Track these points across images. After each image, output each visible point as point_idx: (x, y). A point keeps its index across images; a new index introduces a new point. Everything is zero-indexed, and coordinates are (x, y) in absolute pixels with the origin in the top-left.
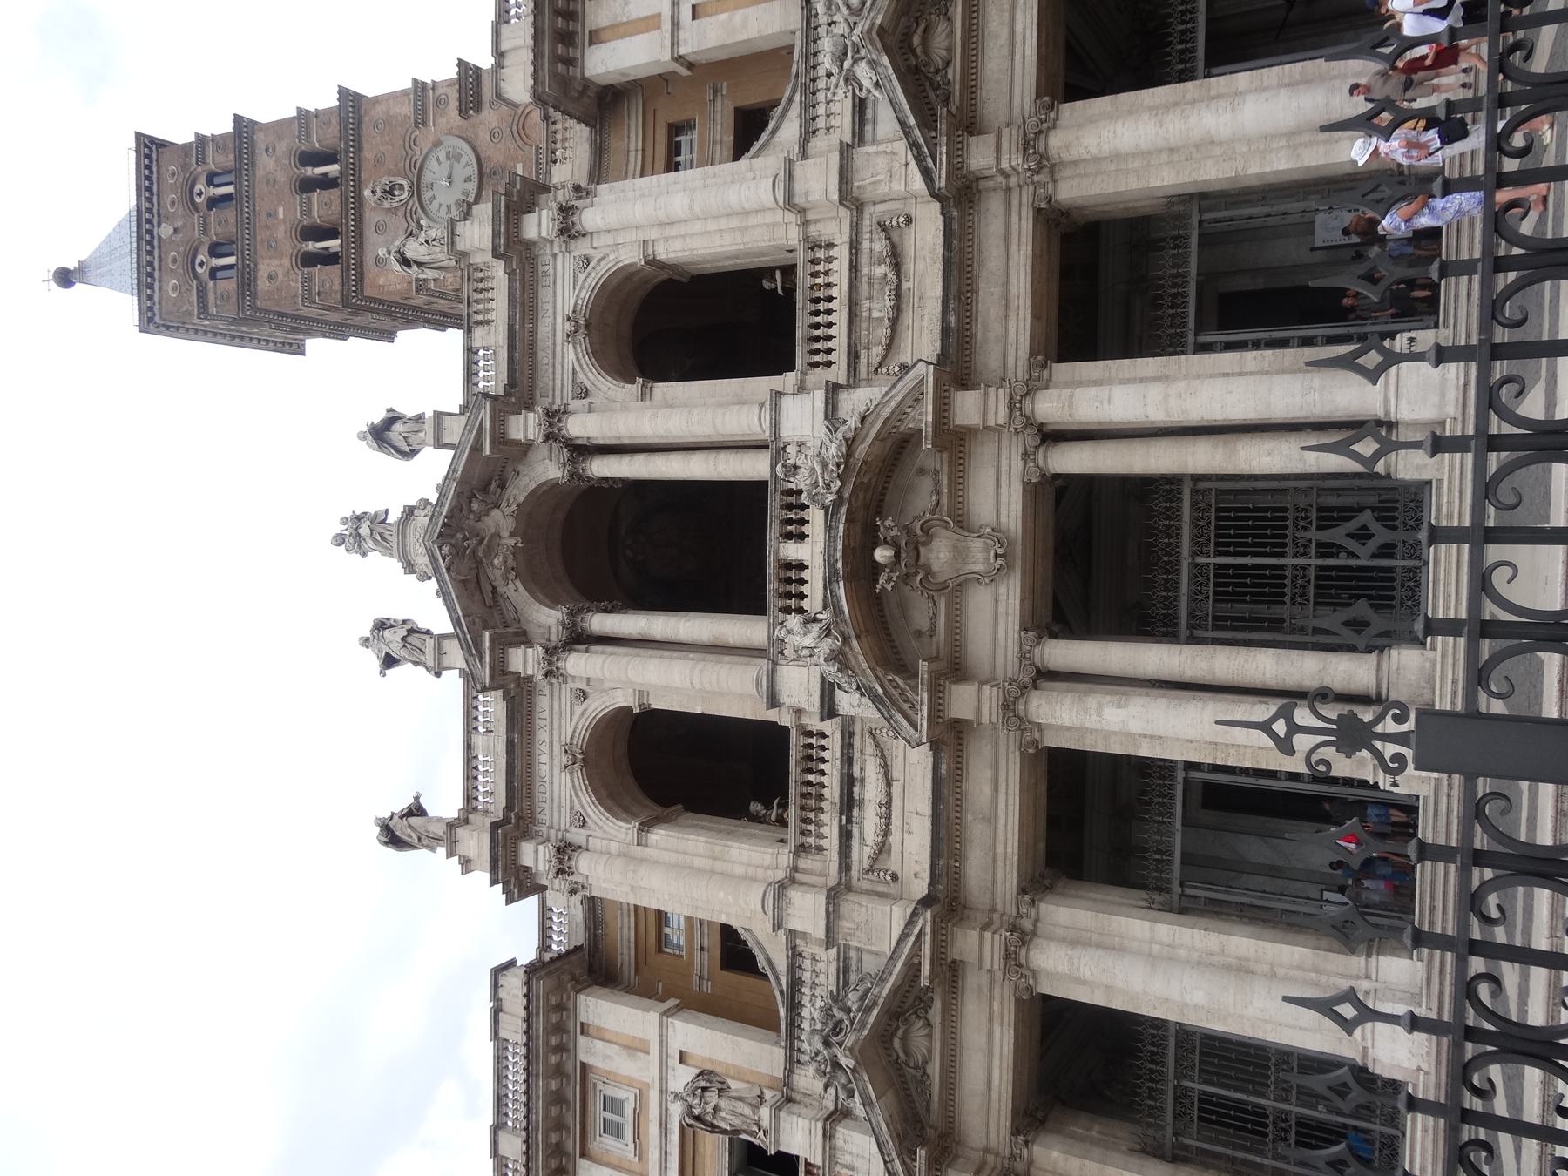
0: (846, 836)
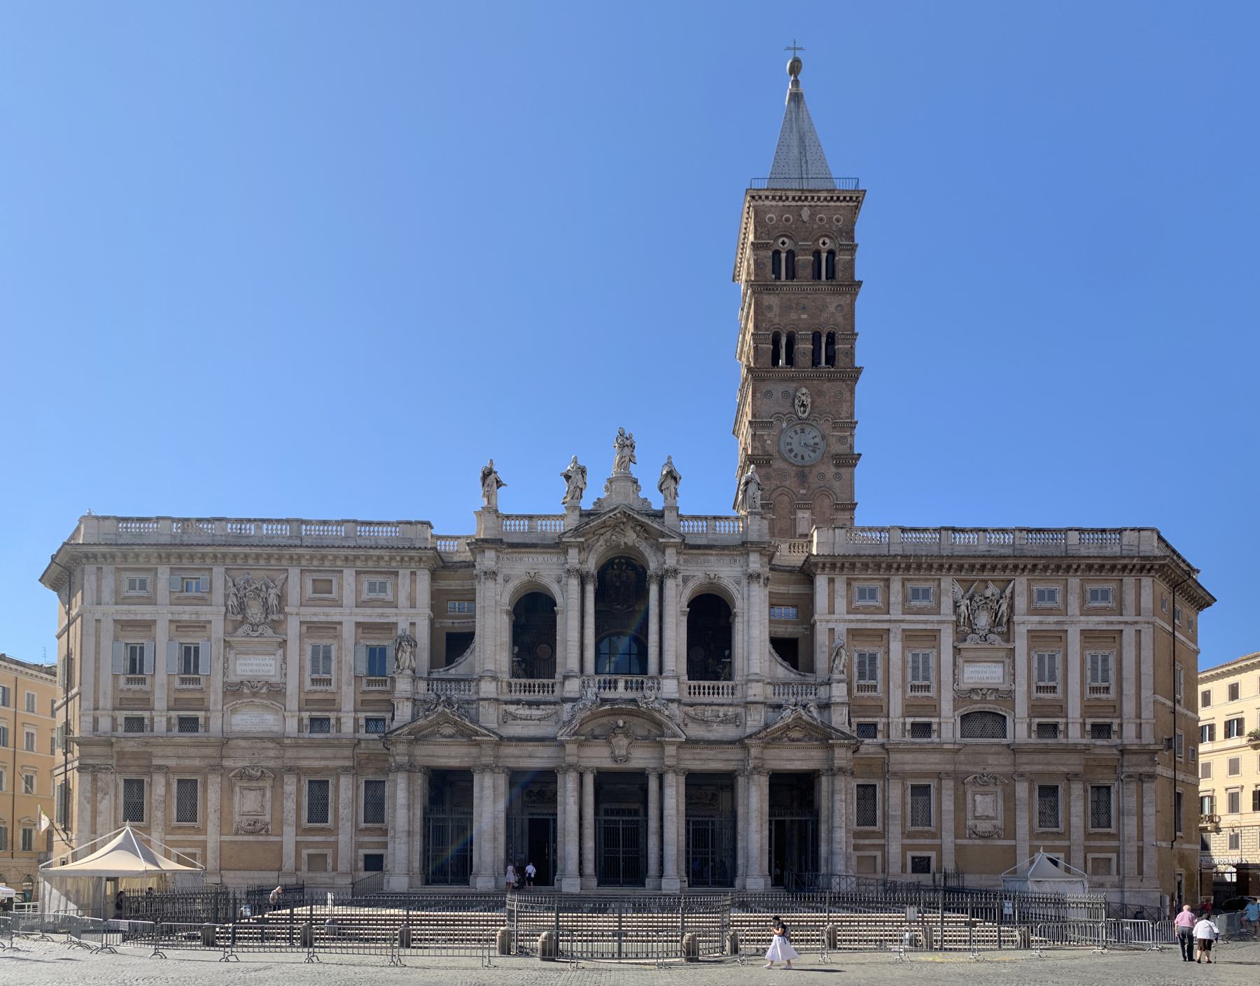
0: (518, 702)
